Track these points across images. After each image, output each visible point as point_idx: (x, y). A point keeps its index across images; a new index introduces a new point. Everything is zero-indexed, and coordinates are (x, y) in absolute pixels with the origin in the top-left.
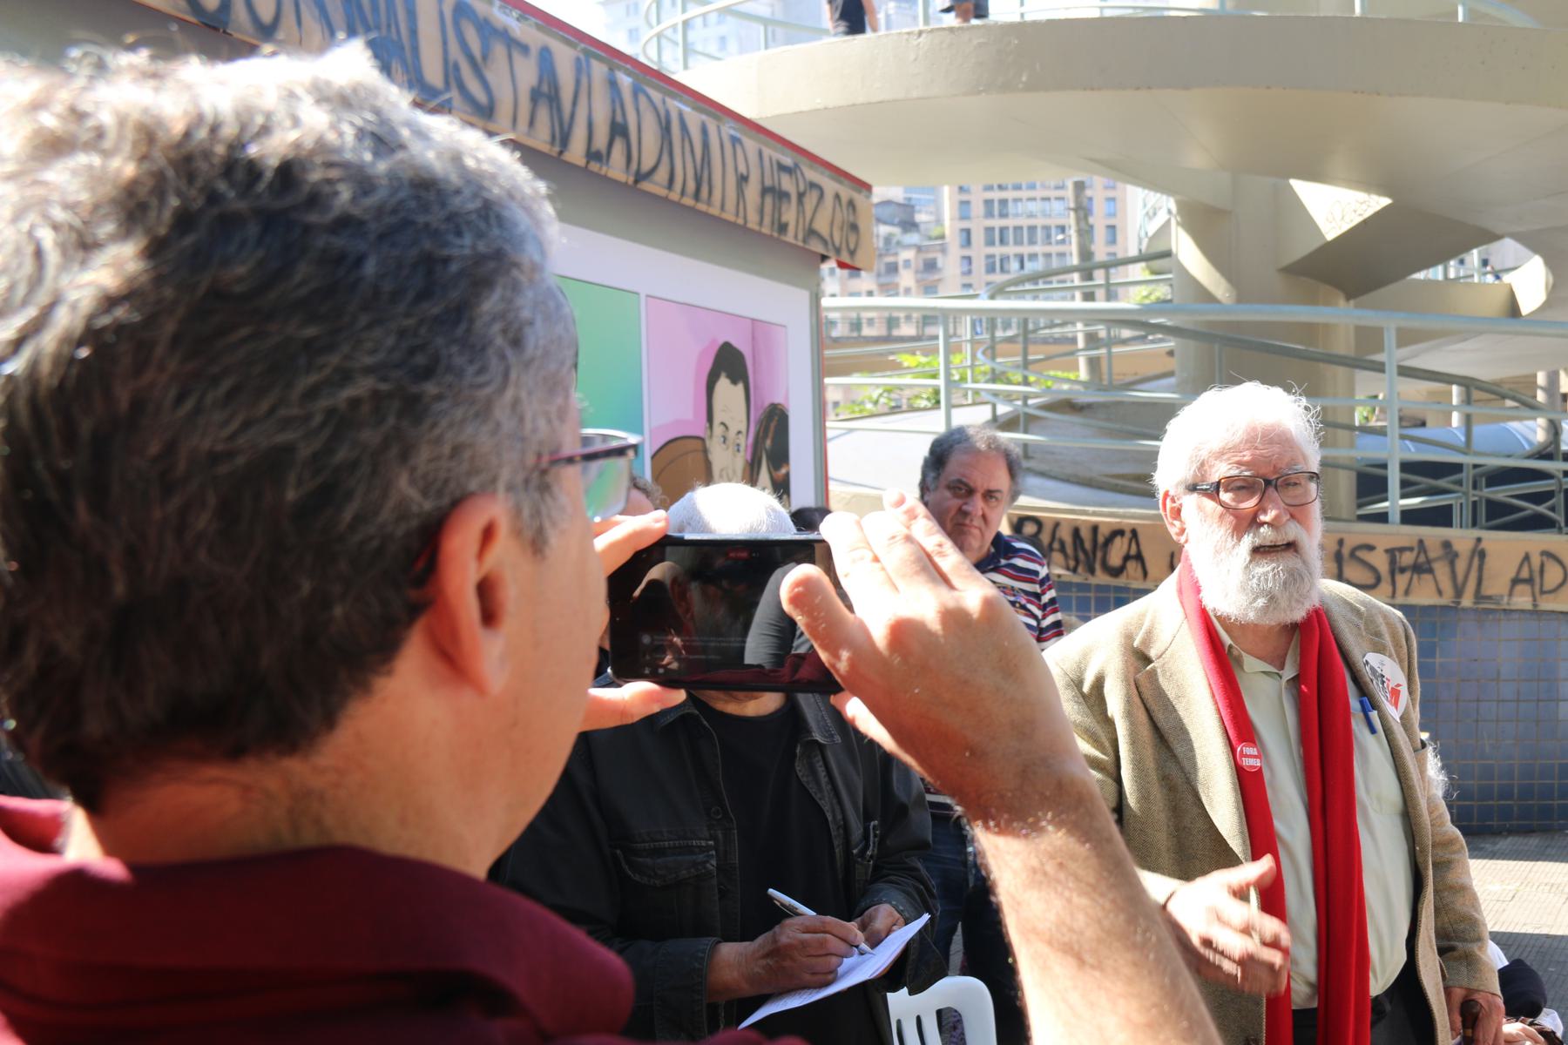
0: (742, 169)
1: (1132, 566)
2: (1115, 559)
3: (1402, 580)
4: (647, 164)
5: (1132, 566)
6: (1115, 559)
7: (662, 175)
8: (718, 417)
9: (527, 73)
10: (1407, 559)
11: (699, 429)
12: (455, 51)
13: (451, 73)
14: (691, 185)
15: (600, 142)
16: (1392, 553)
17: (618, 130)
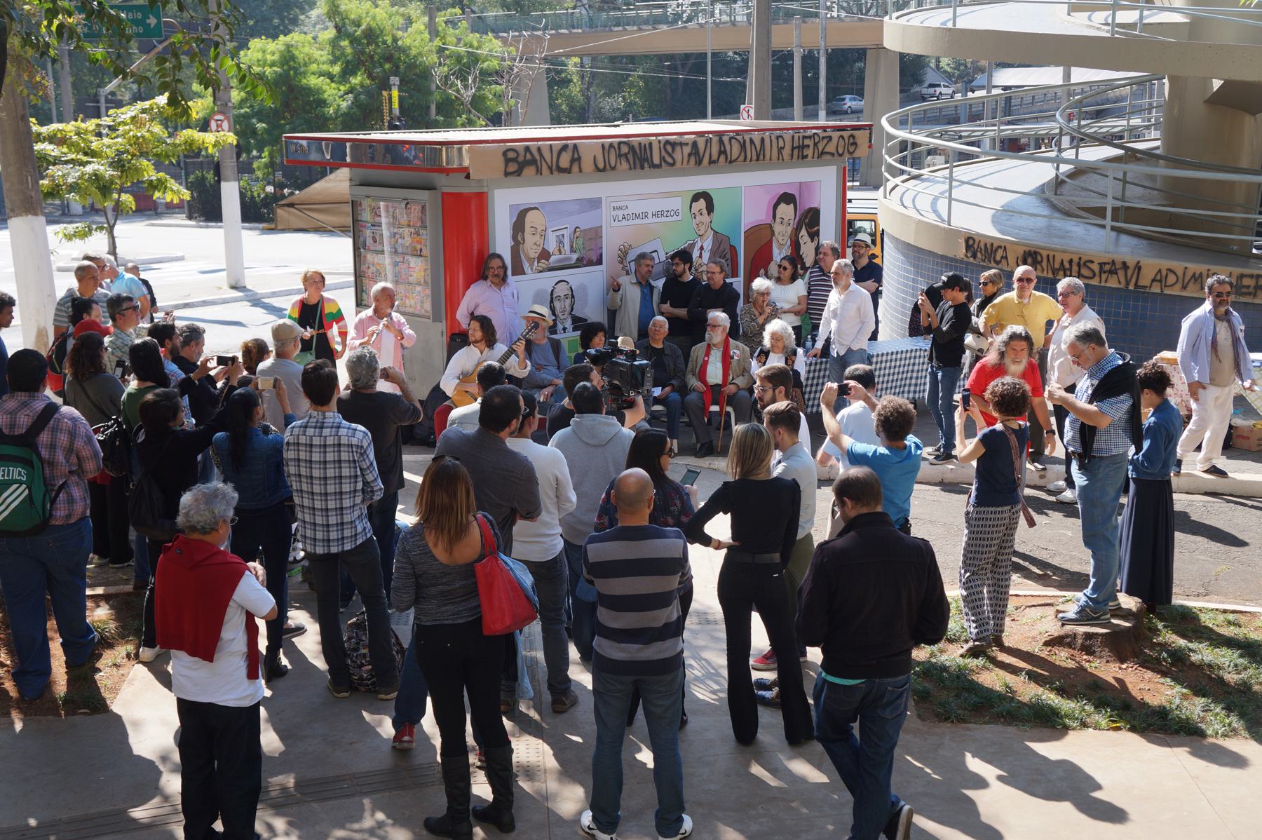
0: (781, 144)
1: (1004, 261)
2: (998, 258)
3: (1104, 276)
4: (734, 157)
5: (1004, 261)
6: (998, 258)
7: (742, 158)
8: (778, 216)
9: (687, 150)
10: (1107, 267)
11: (770, 221)
12: (663, 153)
13: (662, 159)
14: (755, 157)
15: (715, 157)
16: (1100, 264)
17: (722, 152)
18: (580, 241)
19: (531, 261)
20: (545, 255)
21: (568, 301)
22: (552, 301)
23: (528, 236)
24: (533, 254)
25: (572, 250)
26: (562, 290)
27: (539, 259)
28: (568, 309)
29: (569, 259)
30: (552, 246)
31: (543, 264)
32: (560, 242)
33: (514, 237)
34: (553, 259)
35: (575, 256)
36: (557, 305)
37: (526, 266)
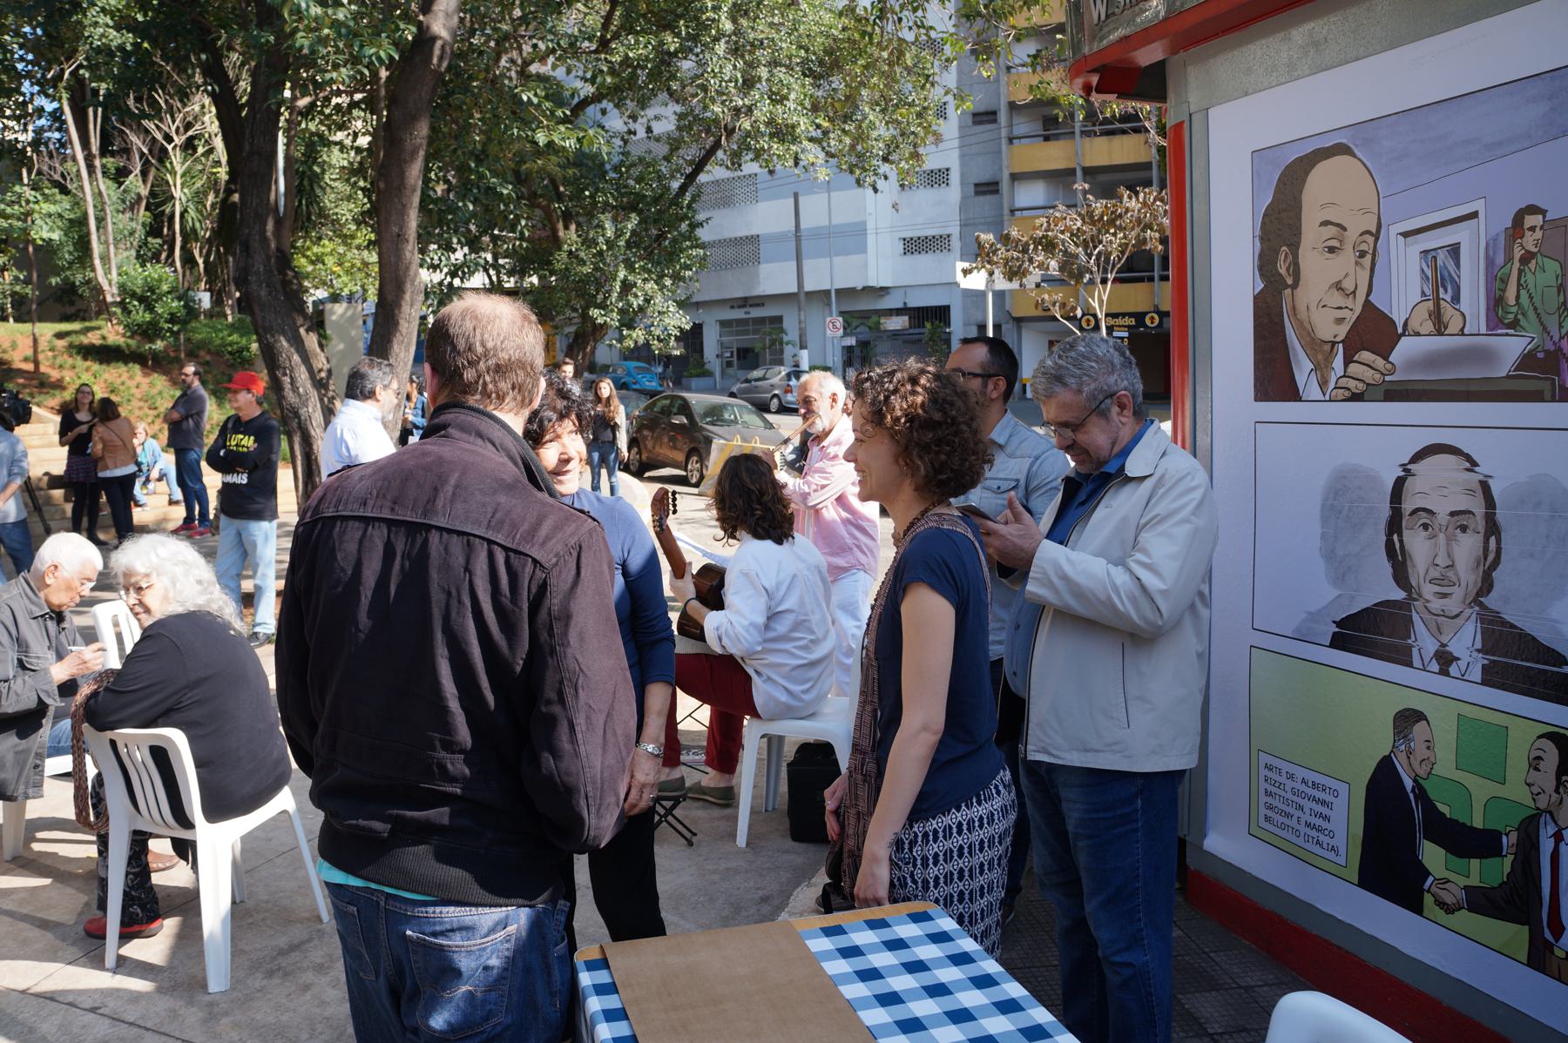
18: (1546, 275)
19: (1321, 352)
20: (1374, 332)
21: (1468, 547)
22: (1395, 524)
23: (1312, 259)
24: (1329, 327)
25: (1500, 316)
26: (1440, 487)
27: (1353, 345)
28: (1468, 576)
29: (1485, 356)
30: (1402, 297)
31: (1368, 366)
32: (1441, 281)
33: (1266, 265)
34: (1405, 349)
35: (1512, 347)
36: (1417, 544)
37: (1303, 369)
